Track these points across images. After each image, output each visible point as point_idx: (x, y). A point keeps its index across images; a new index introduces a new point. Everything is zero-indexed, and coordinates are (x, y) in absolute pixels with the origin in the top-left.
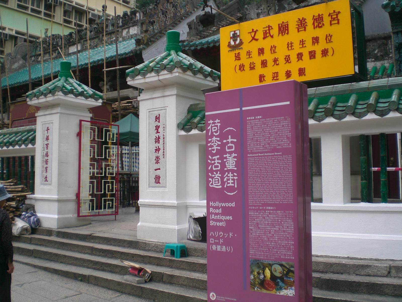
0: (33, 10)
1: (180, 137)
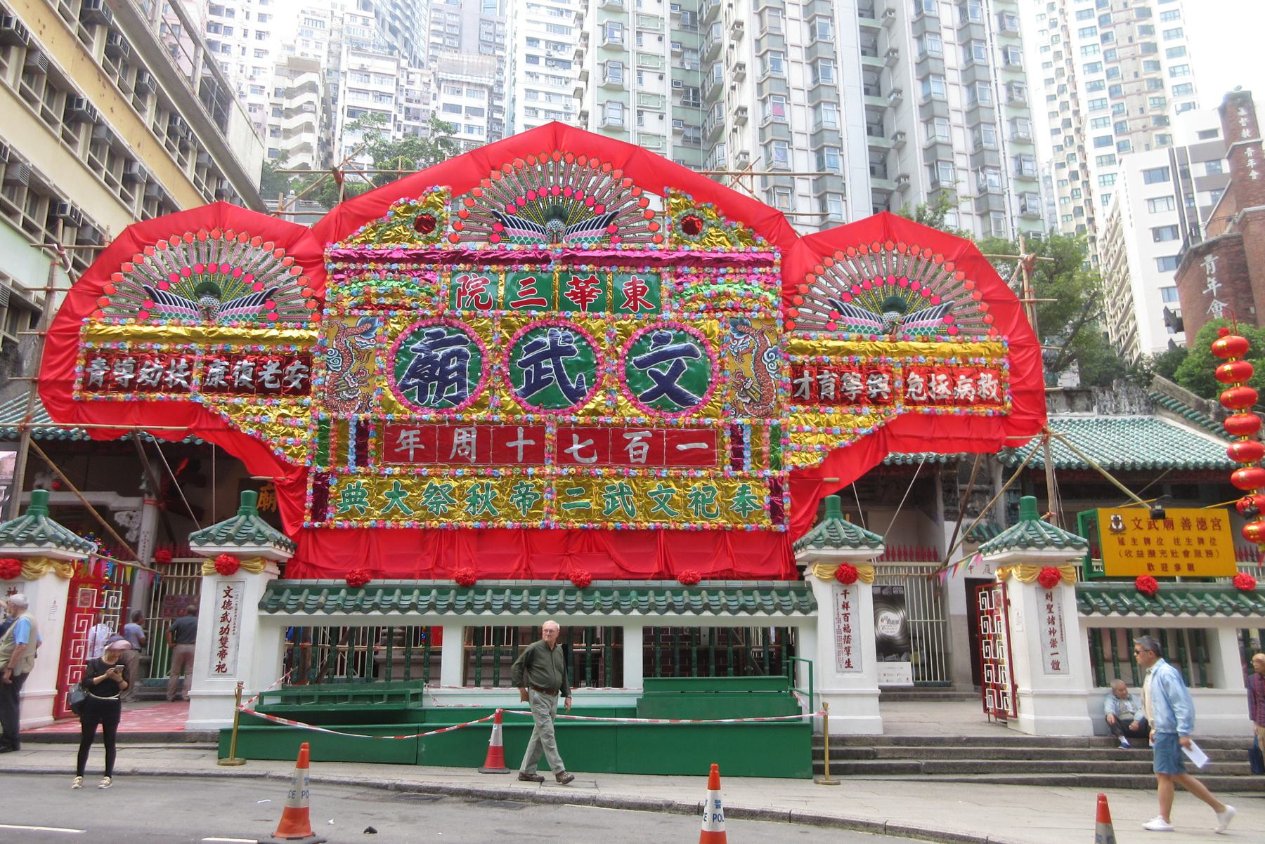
0: (26, 225)
1: (1079, 618)
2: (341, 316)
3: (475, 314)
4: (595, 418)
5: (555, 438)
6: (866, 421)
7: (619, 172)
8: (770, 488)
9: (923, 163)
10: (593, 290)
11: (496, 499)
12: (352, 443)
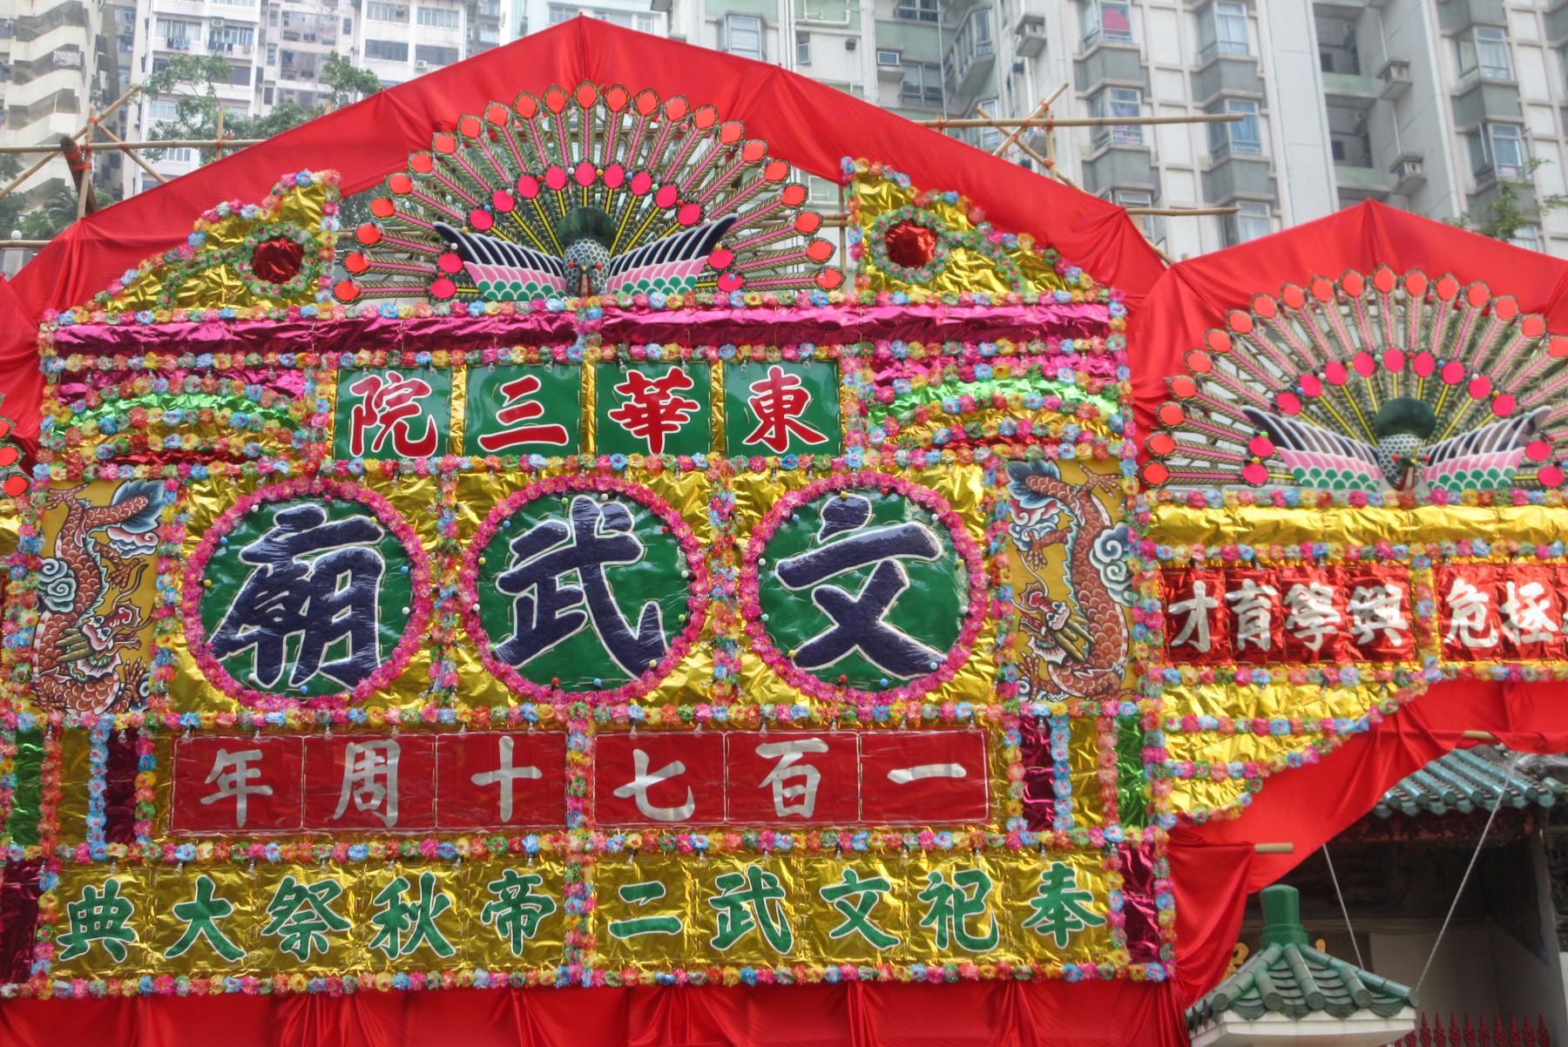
2: (76, 478)
3: (396, 470)
4: (688, 709)
5: (589, 761)
7: (734, 128)
8: (1123, 871)
9: (1453, 129)
10: (677, 404)
11: (448, 915)
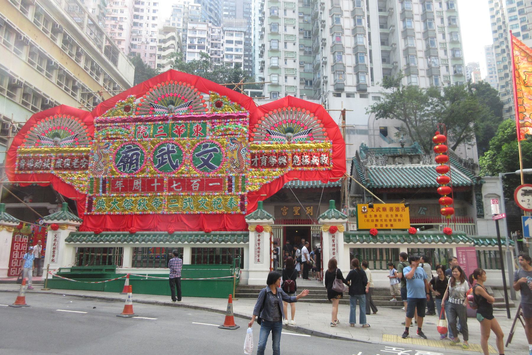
2: (99, 142)
3: (142, 140)
6: (277, 173)
7: (193, 87)
9: (403, 56)
10: (183, 130)
12: (101, 186)
